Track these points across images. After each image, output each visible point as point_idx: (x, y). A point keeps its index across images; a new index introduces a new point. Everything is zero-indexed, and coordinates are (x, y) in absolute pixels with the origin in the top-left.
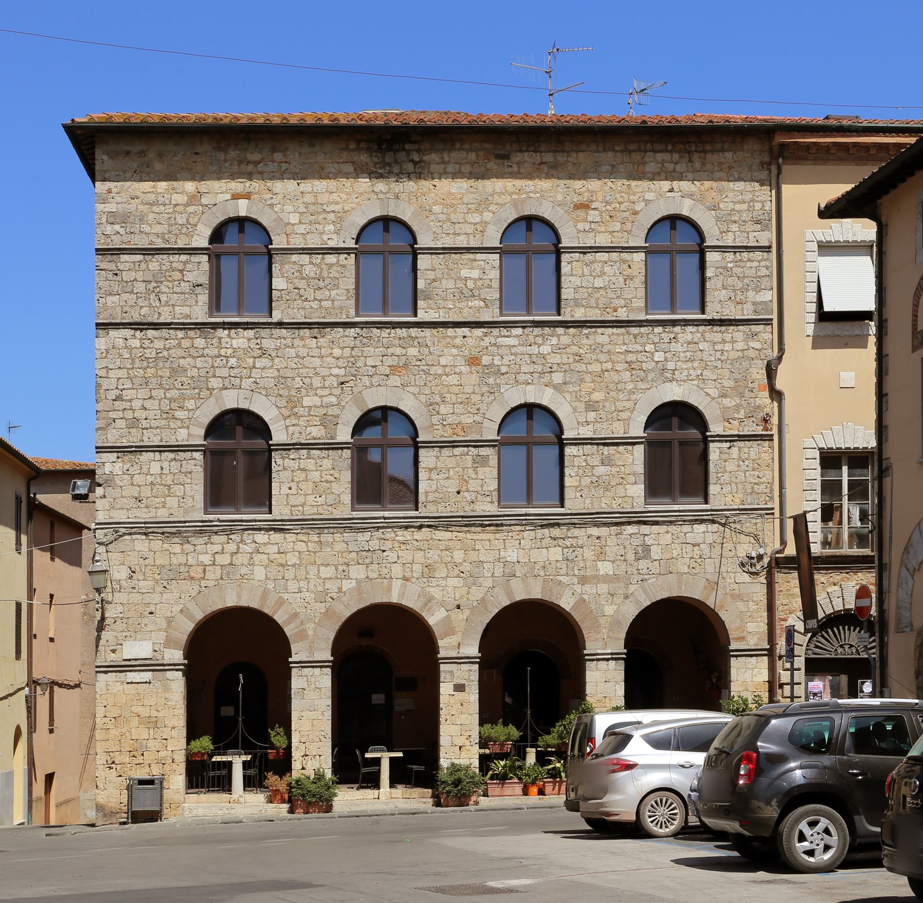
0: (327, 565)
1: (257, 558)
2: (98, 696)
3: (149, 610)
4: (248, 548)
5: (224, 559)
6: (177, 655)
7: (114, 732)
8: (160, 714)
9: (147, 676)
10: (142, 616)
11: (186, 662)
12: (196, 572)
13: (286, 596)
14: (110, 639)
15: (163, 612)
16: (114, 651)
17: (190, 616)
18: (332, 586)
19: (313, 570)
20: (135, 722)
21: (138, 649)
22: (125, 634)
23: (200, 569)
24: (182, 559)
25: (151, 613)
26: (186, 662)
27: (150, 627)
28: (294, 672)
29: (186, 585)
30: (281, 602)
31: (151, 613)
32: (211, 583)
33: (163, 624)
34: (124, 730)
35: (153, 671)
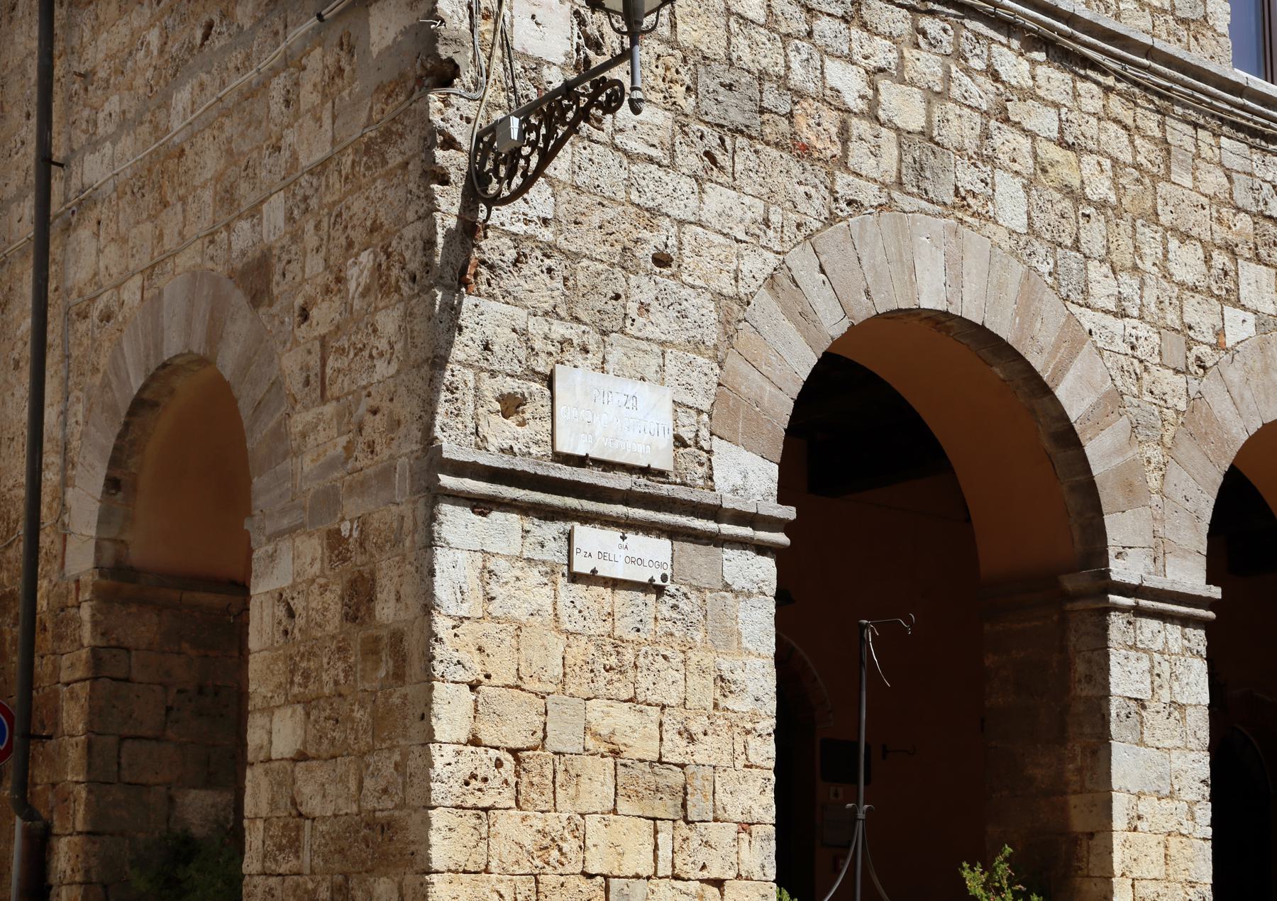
0: (1185, 237)
1: (1006, 141)
2: (442, 625)
3: (655, 240)
4: (980, 92)
5: (904, 107)
6: (748, 476)
7: (513, 829)
8: (703, 752)
9: (647, 555)
10: (626, 261)
11: (789, 513)
12: (817, 128)
13: (1088, 319)
14: (503, 338)
15: (706, 263)
16: (511, 405)
17: (804, 317)
18: (1200, 314)
19: (1150, 238)
20: (597, 781)
21: (616, 415)
22: (560, 330)
23: (830, 121)
24: (770, 58)
25: (662, 260)
26: (789, 513)
27: (661, 324)
28: (1117, 622)
29: (785, 174)
30: (1075, 338)
31: (662, 260)
32: (869, 194)
33: (704, 311)
34: (554, 823)
35: (673, 533)
